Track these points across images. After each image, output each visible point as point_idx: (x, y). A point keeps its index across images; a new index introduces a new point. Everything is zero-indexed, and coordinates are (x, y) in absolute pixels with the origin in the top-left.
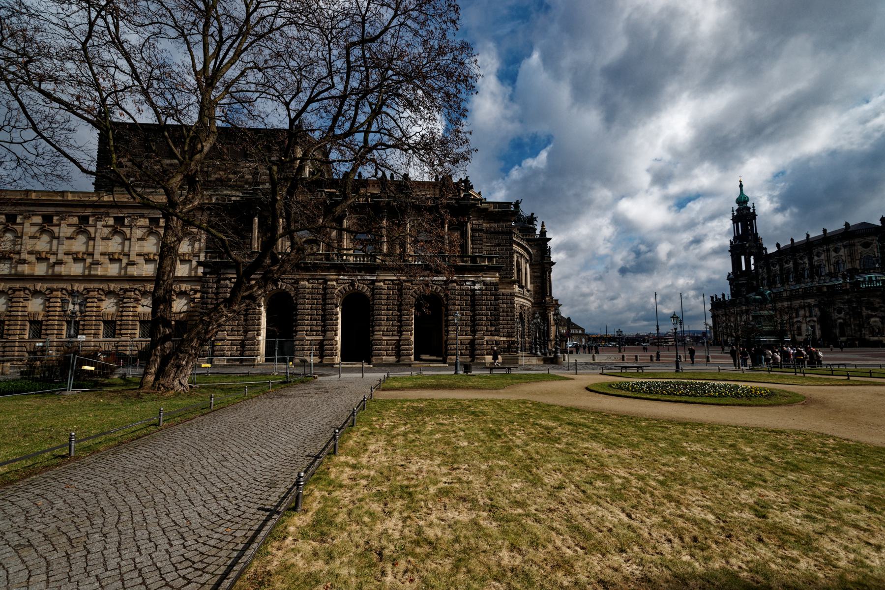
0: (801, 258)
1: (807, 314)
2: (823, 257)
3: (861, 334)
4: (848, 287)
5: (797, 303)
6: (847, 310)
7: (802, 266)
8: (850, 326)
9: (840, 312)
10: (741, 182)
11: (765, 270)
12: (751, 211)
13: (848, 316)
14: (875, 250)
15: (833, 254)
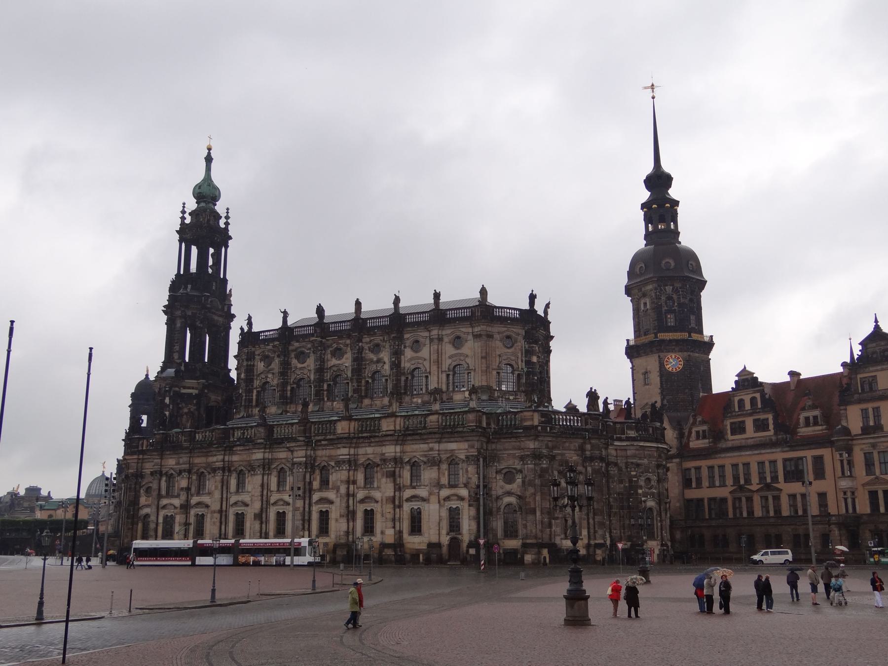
0: (376, 348)
1: (444, 480)
2: (425, 352)
3: (551, 531)
4: (536, 423)
5: (417, 450)
6: (531, 476)
7: (374, 367)
8: (534, 512)
9: (509, 477)
10: (209, 149)
11: (276, 365)
12: (222, 225)
13: (531, 490)
14: (520, 355)
15: (449, 350)
